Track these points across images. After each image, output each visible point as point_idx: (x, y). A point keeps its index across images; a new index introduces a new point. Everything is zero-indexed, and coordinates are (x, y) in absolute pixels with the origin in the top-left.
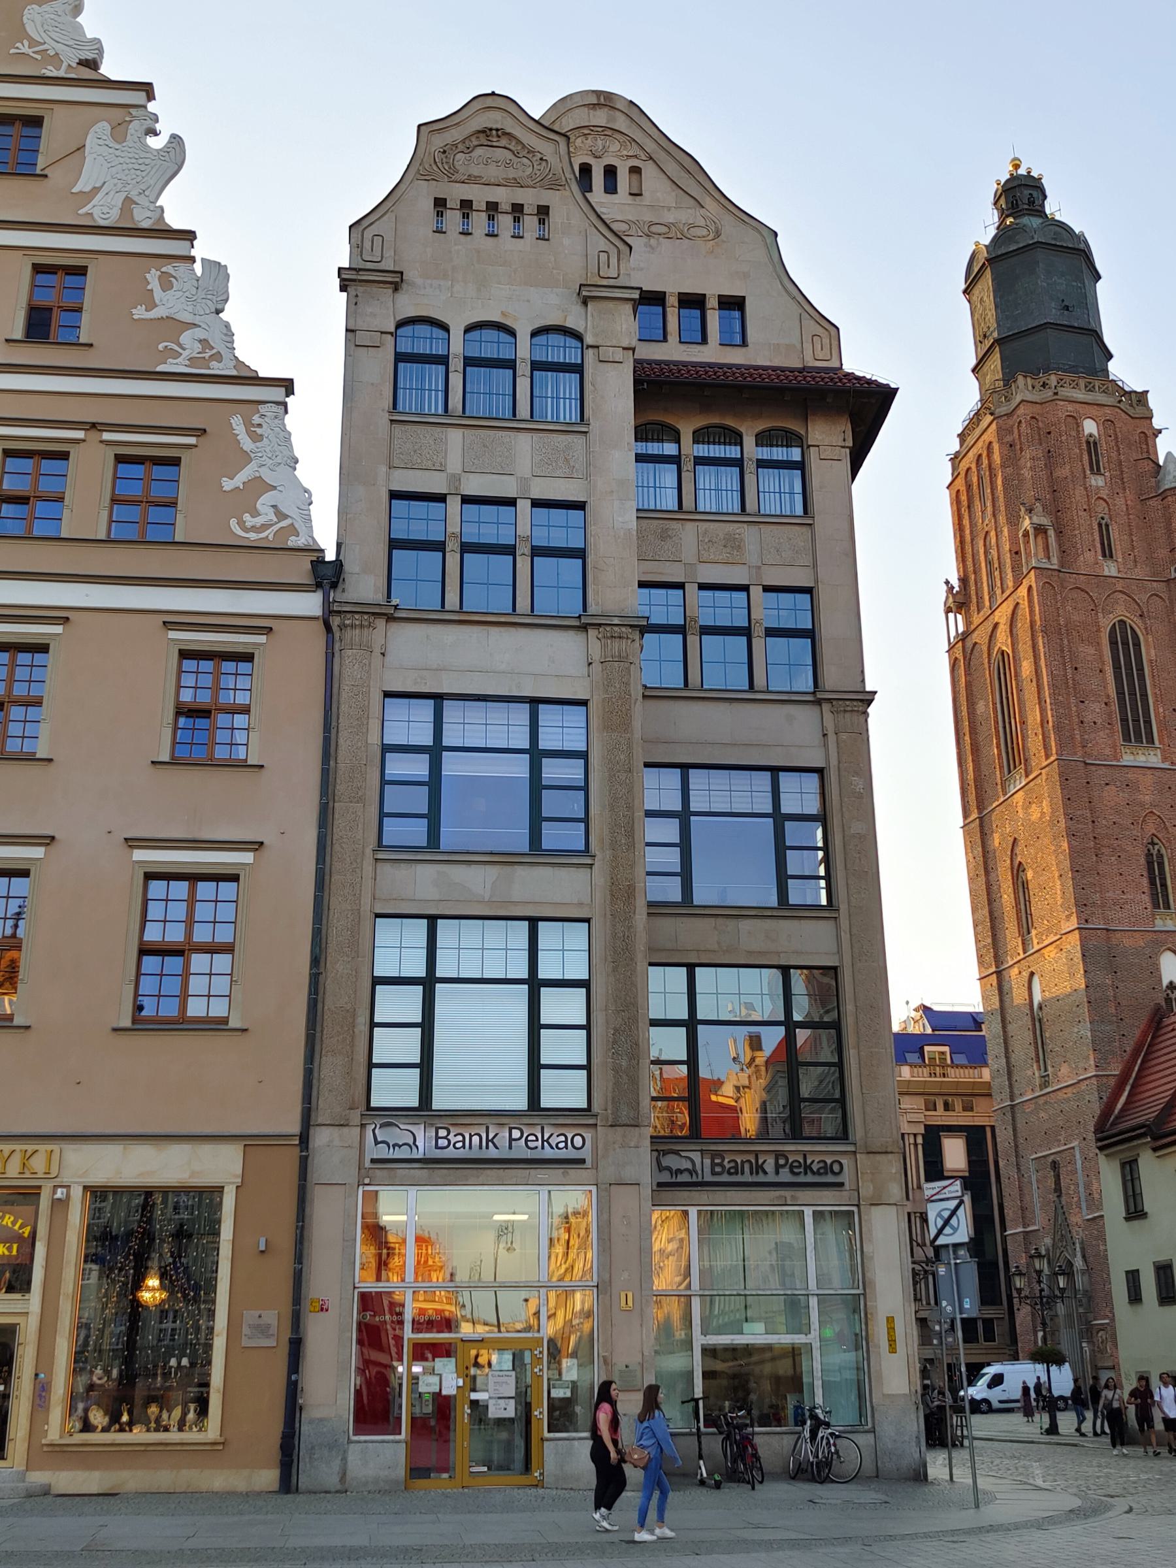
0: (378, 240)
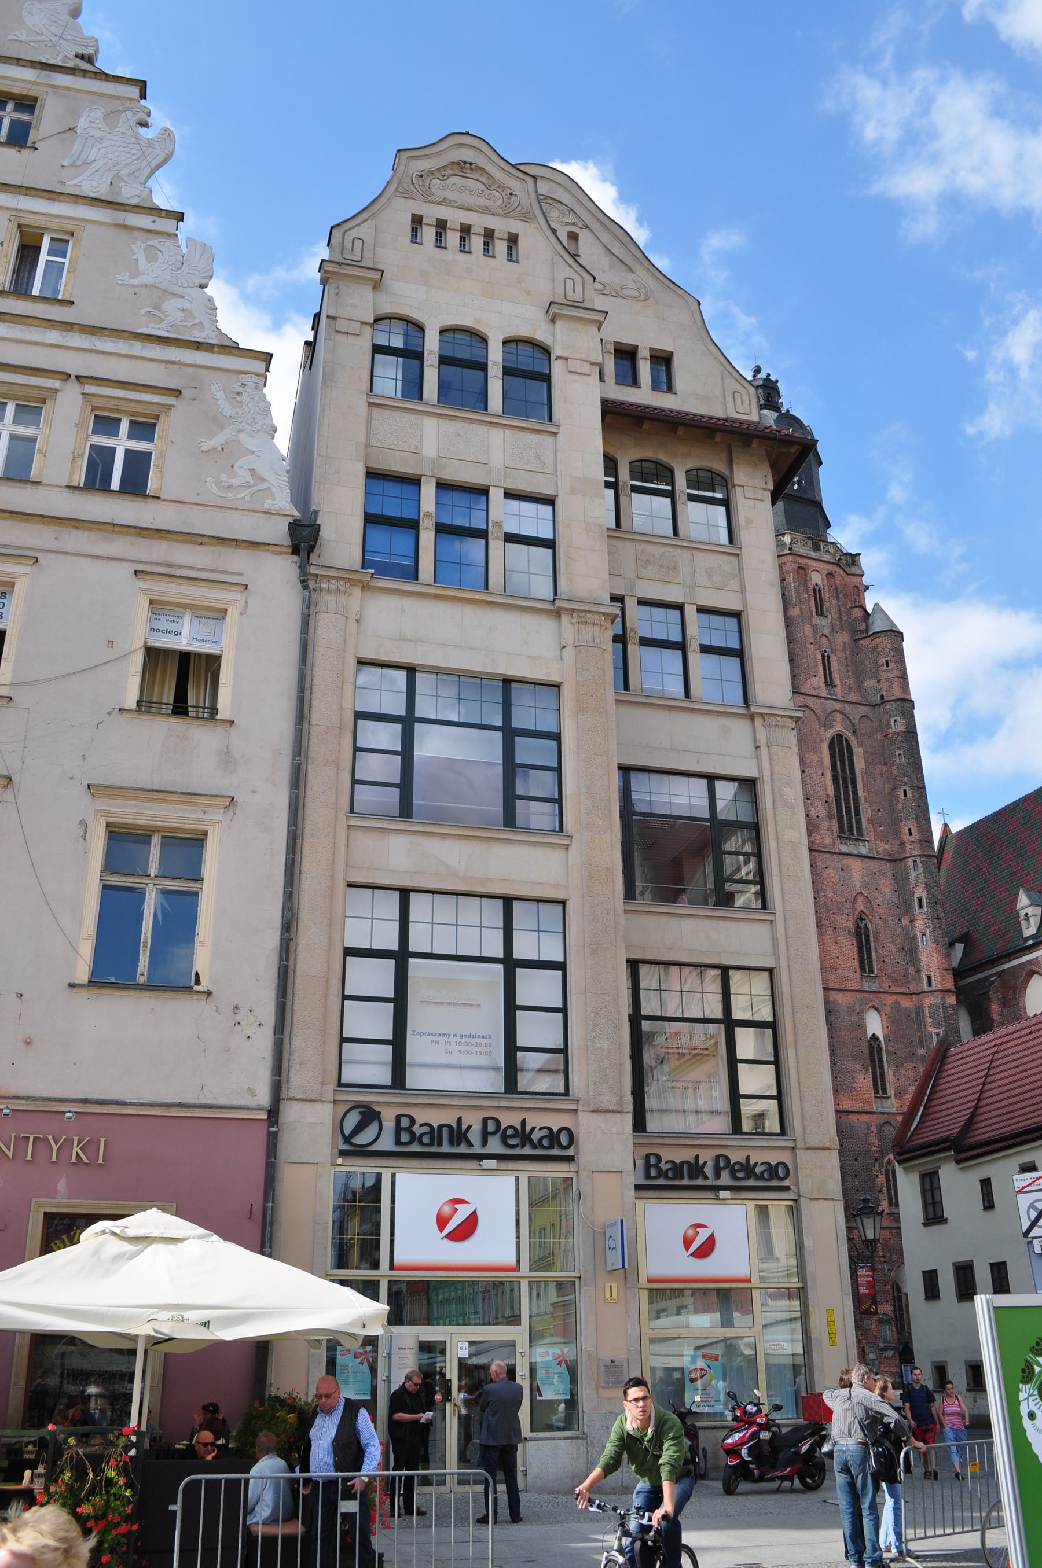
0: (358, 244)
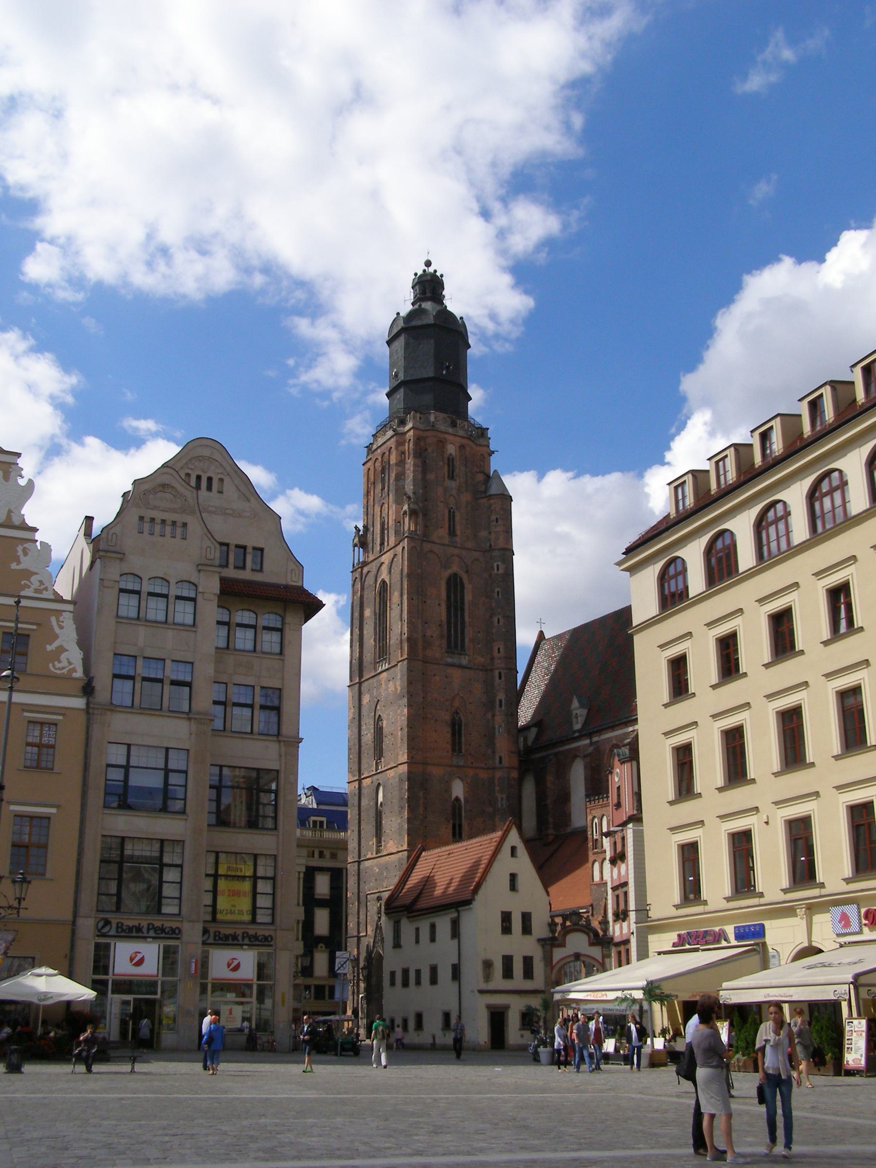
0: (114, 536)
